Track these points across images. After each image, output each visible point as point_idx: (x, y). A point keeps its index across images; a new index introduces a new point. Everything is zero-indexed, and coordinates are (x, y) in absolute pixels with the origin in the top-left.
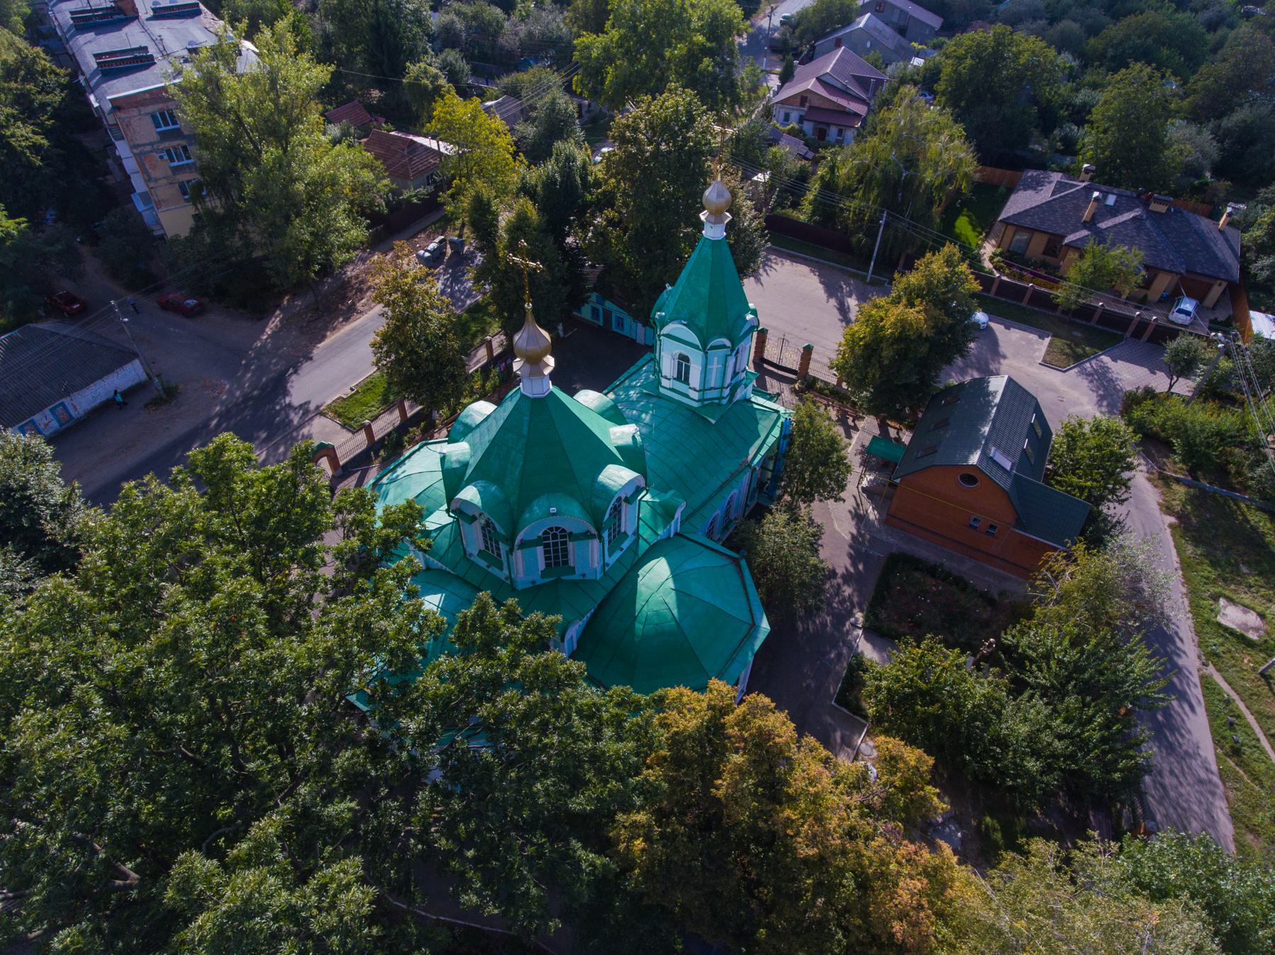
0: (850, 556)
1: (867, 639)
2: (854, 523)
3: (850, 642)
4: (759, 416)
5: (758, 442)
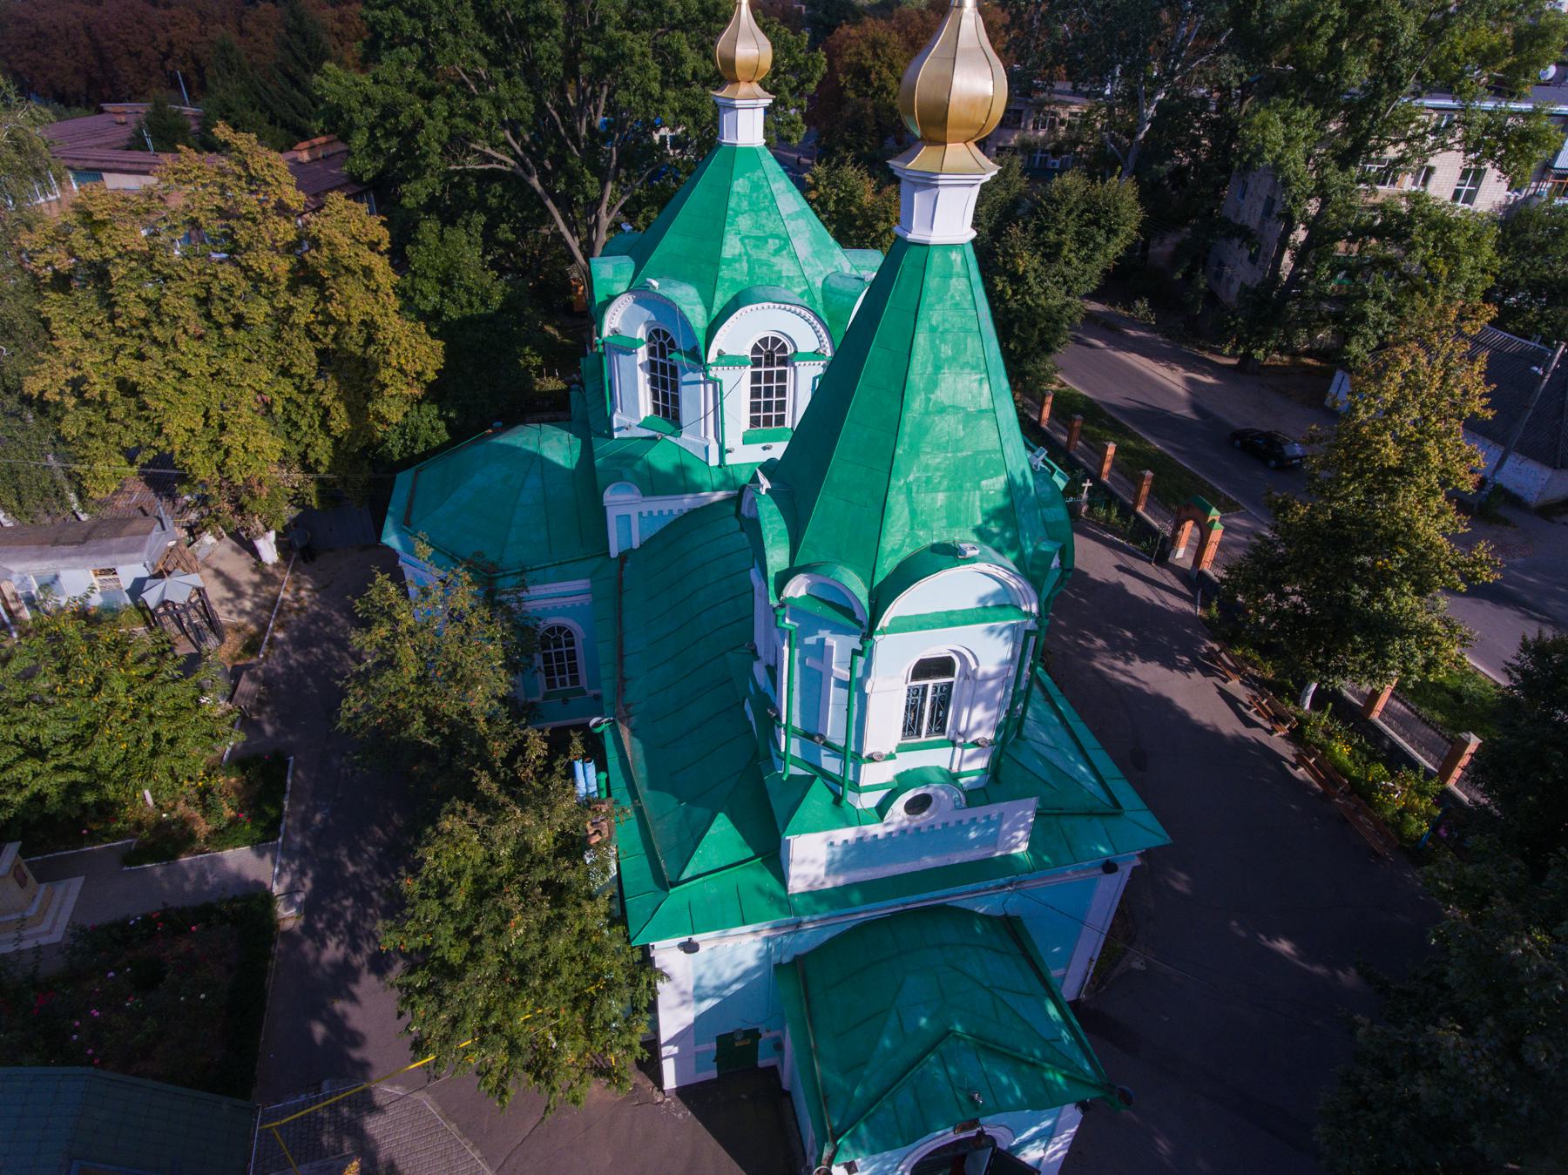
0: (356, 1039)
1: (259, 885)
2: (382, 1156)
3: (291, 859)
4: (699, 812)
5: (641, 775)
